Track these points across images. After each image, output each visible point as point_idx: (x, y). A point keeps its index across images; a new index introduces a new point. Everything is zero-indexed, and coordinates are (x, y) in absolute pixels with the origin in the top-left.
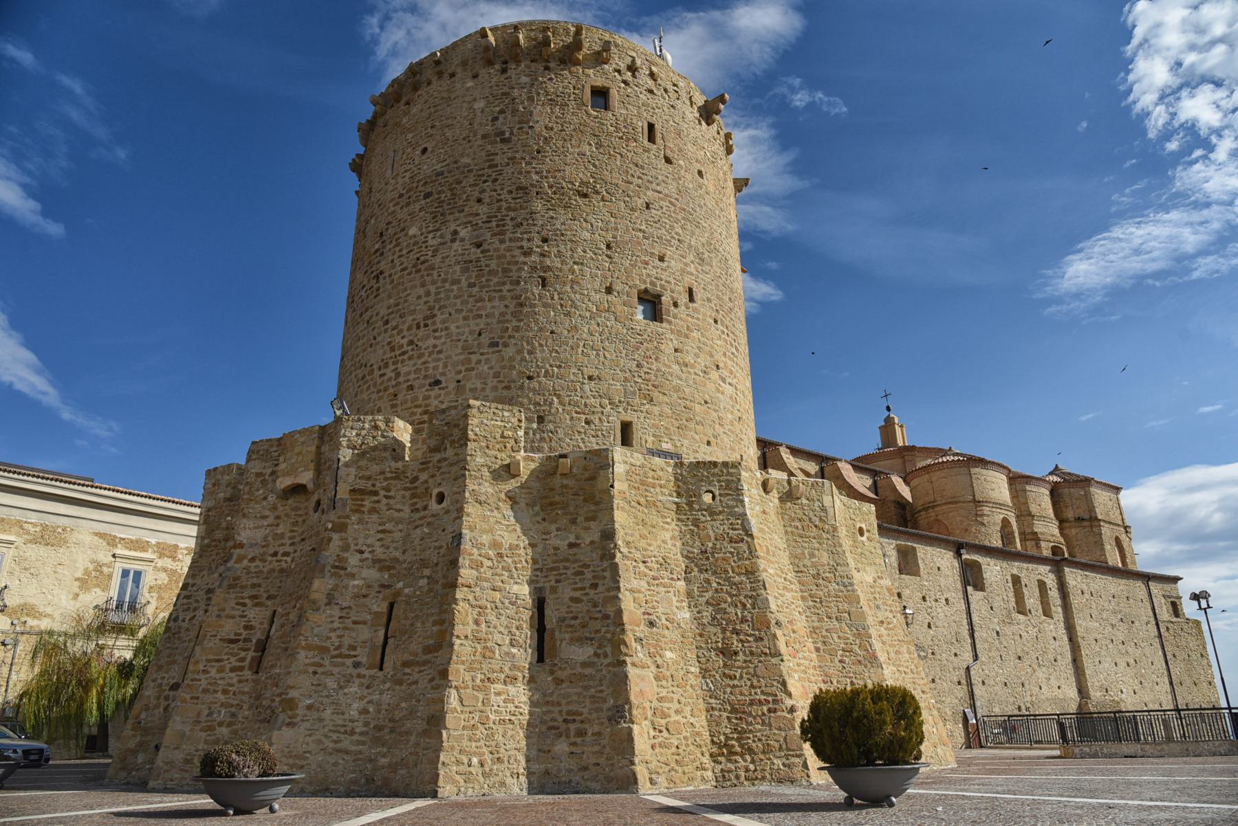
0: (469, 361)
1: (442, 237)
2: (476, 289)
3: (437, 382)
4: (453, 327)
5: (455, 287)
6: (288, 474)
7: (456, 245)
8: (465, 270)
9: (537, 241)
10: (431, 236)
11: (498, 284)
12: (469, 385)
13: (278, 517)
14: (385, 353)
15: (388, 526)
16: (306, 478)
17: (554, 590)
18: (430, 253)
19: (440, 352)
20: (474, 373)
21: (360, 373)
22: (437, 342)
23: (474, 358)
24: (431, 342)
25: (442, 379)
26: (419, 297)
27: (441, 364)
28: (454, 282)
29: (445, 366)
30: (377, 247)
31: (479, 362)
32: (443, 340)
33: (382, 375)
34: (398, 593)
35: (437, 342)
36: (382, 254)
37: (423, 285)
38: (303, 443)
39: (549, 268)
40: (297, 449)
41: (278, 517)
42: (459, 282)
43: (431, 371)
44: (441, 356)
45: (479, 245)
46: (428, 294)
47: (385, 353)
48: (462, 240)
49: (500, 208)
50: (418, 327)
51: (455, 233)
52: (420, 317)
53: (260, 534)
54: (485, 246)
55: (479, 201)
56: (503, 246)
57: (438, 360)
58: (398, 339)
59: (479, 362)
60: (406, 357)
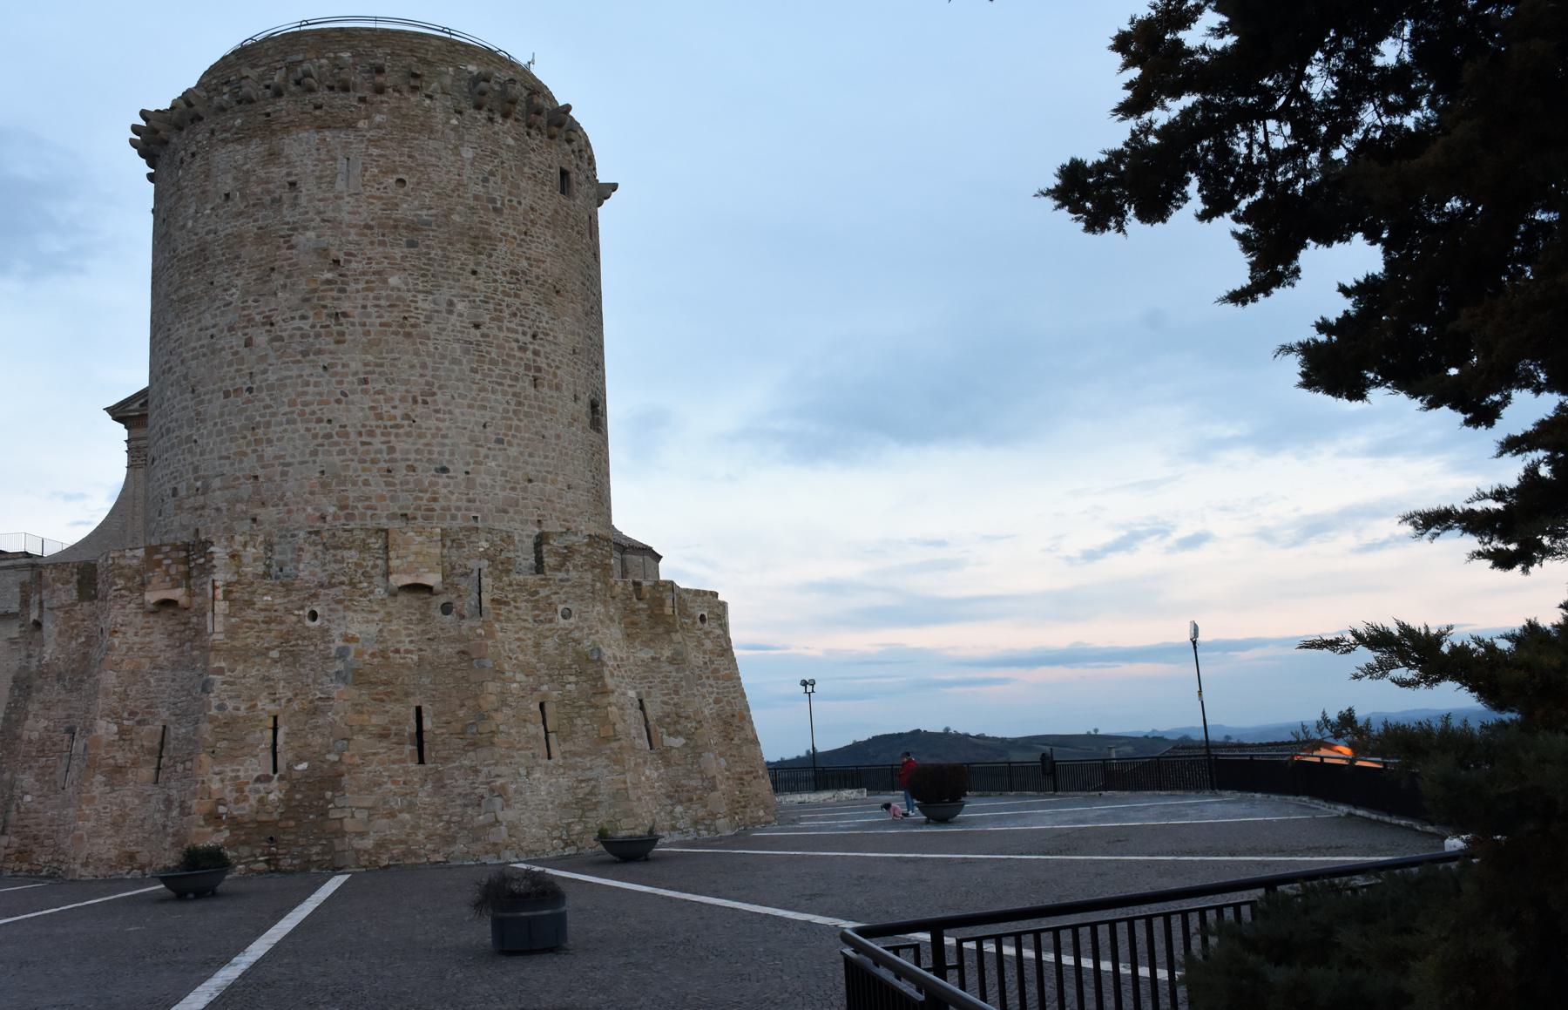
0: (477, 454)
1: (435, 302)
2: (478, 377)
3: (444, 470)
4: (457, 411)
5: (456, 368)
6: (405, 572)
7: (454, 318)
8: (467, 352)
9: (529, 338)
10: (421, 296)
11: (499, 376)
12: (479, 480)
13: (389, 613)
14: (367, 418)
15: (521, 635)
16: (433, 579)
17: (649, 694)
18: (422, 318)
19: (444, 436)
20: (482, 468)
21: (320, 429)
22: (441, 425)
23: (483, 451)
24: (432, 423)
25: (451, 468)
26: (412, 367)
27: (447, 449)
28: (454, 361)
29: (452, 454)
30: (329, 276)
31: (487, 457)
32: (447, 423)
33: (363, 443)
34: (545, 695)
35: (441, 425)
36: (343, 291)
37: (416, 353)
38: (422, 543)
39: (539, 369)
40: (414, 548)
41: (389, 613)
42: (459, 363)
43: (435, 456)
44: (447, 441)
45: (477, 326)
46: (424, 366)
47: (367, 418)
48: (461, 315)
49: (496, 290)
50: (415, 401)
51: (451, 303)
52: (416, 390)
53: (373, 629)
54: (484, 329)
55: (474, 273)
56: (501, 335)
57: (444, 445)
58: (386, 408)
59: (487, 457)
60: (401, 431)
